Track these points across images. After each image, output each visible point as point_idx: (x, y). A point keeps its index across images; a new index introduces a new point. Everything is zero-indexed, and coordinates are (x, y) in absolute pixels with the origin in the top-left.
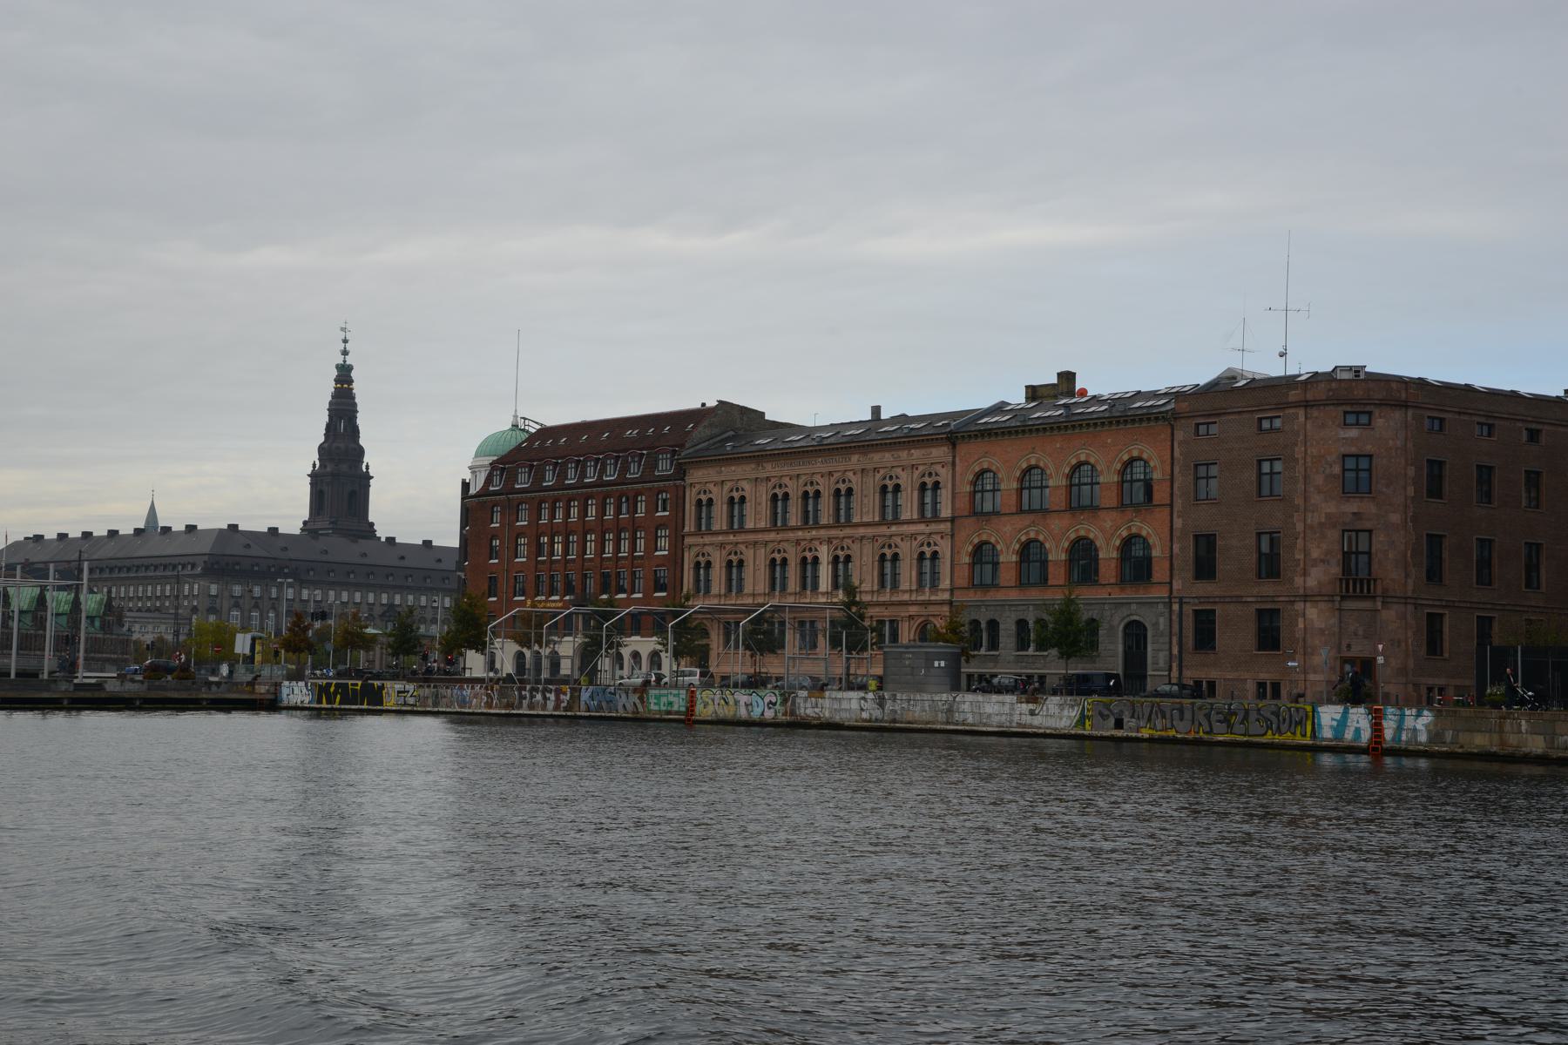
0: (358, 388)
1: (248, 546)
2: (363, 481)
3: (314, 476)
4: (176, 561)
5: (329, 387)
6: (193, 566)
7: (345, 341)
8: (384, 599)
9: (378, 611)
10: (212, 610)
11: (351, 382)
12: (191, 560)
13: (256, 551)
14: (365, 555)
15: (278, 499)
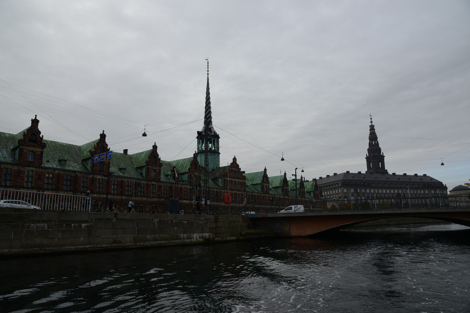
0: (377, 131)
1: (353, 177)
2: (381, 158)
3: (367, 158)
4: (332, 183)
5: (368, 132)
6: (338, 184)
7: (371, 119)
8: (396, 191)
9: (395, 196)
10: (345, 197)
11: (374, 130)
12: (337, 182)
13: (355, 178)
14: (388, 178)
15: (359, 165)
